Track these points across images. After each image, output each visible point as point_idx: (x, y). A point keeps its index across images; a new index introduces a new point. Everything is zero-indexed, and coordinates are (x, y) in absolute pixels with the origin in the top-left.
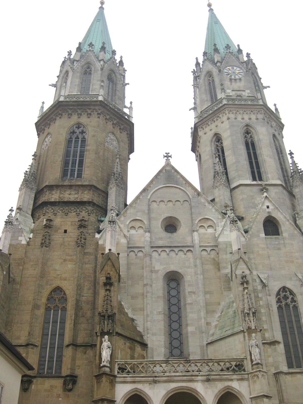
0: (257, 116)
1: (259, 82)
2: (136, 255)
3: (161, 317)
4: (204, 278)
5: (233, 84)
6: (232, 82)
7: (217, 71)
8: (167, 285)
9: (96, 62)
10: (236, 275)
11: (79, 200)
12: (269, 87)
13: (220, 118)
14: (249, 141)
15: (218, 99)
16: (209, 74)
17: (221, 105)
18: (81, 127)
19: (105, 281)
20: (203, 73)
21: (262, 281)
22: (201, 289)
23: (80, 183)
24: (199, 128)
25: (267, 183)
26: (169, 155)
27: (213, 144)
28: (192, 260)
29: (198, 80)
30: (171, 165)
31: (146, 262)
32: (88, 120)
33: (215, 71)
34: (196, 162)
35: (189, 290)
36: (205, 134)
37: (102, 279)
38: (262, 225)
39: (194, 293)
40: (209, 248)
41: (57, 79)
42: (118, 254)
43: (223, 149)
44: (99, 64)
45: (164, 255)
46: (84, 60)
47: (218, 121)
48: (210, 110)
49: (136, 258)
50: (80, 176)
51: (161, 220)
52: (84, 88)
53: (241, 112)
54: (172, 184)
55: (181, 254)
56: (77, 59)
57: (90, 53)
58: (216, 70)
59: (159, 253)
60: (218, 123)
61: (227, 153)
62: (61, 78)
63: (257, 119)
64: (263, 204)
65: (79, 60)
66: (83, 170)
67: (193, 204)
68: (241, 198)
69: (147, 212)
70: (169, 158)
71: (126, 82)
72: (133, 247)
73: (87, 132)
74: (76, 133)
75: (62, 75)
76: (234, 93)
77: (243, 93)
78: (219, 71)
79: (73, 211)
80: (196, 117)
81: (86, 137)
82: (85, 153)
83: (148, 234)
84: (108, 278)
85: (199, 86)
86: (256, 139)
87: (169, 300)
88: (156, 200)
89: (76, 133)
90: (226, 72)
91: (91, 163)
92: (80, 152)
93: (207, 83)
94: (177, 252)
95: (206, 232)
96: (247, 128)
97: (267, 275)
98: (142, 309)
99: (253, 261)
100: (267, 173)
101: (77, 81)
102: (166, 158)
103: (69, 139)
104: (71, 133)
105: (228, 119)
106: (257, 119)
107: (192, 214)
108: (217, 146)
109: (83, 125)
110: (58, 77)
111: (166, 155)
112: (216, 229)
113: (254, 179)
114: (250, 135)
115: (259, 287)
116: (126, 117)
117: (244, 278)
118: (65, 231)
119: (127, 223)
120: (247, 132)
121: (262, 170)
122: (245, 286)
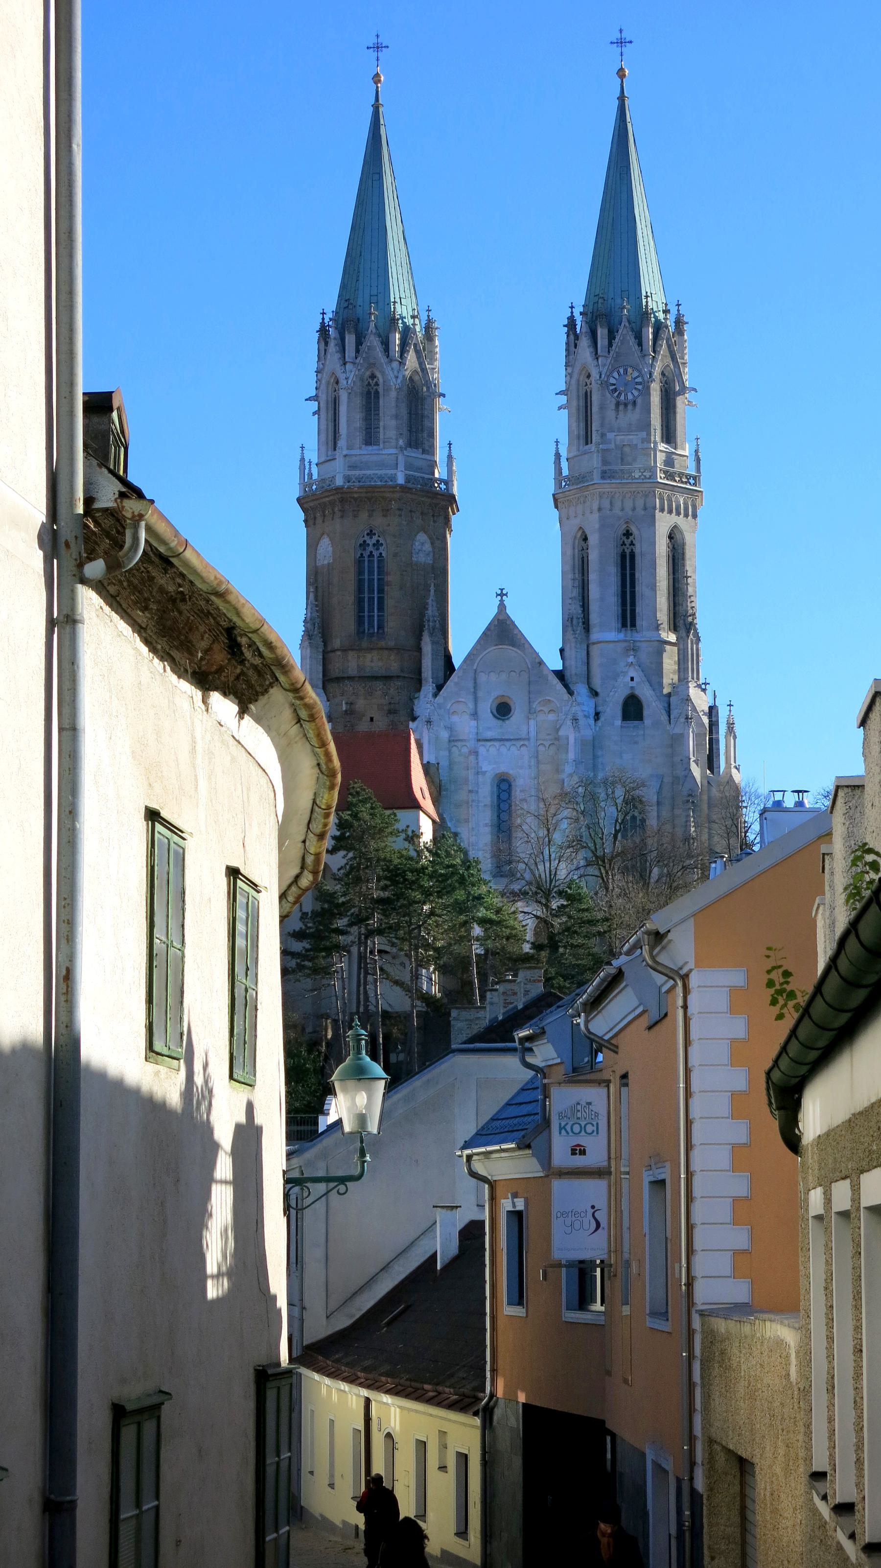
2: (460, 751)
3: (488, 830)
5: (621, 414)
14: (628, 551)
26: (504, 592)
27: (577, 541)
42: (438, 764)
45: (493, 750)
55: (513, 749)
64: (625, 673)
69: (472, 690)
72: (456, 741)
86: (637, 550)
87: (499, 806)
93: (582, 393)
98: (467, 821)
99: (600, 760)
102: (499, 598)
105: (600, 509)
111: (499, 592)
113: (624, 625)
118: (372, 719)
120: (628, 534)
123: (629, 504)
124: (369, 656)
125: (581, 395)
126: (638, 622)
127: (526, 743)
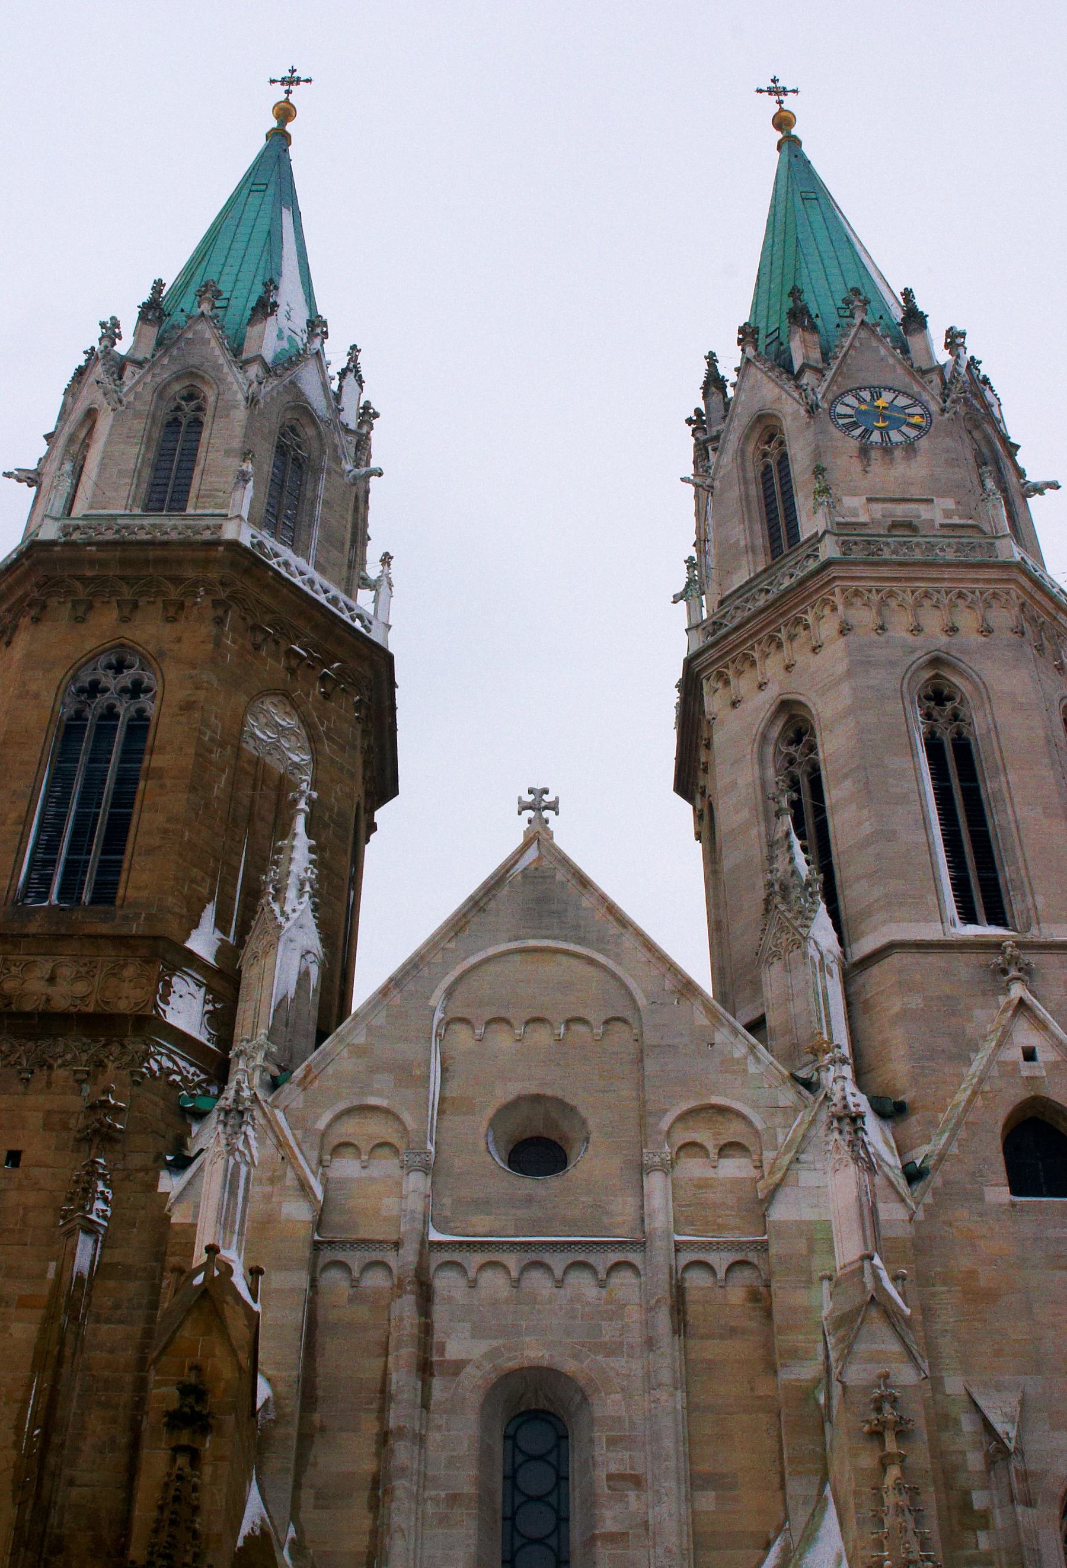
0: (984, 619)
1: (1006, 461)
2: (355, 1283)
4: (691, 1407)
6: (869, 460)
7: (803, 412)
8: (506, 1437)
9: (226, 369)
10: (845, 1387)
11: (91, 1009)
12: (1055, 486)
13: (807, 627)
14: (947, 738)
15: (802, 540)
16: (767, 428)
17: (812, 565)
18: (131, 667)
19: (175, 1405)
20: (736, 423)
21: (987, 1426)
22: (672, 1464)
23: (104, 929)
24: (708, 679)
25: (1029, 937)
27: (770, 750)
28: (634, 1315)
29: (710, 452)
30: (553, 846)
31: (401, 1319)
32: (167, 631)
33: (791, 412)
34: (698, 846)
35: (613, 1468)
36: (734, 704)
37: (164, 1394)
38: (998, 1143)
39: (637, 1481)
40: (724, 1254)
41: (43, 448)
43: (819, 778)
44: (240, 376)
45: (494, 1283)
46: (173, 360)
47: (795, 644)
48: (761, 590)
49: (351, 1300)
50: (105, 893)
51: (490, 1112)
52: (162, 488)
53: (910, 599)
54: (555, 938)
56: (140, 356)
57: (201, 326)
58: (796, 405)
59: (471, 1274)
60: (798, 652)
61: (834, 792)
62: (62, 441)
63: (987, 631)
65: (146, 360)
66: (126, 865)
67: (650, 1038)
68: (896, 1009)
70: (546, 814)
71: (374, 464)
72: (343, 1244)
73: (158, 688)
74: (106, 690)
75: (67, 430)
76: (878, 509)
77: (924, 512)
78: (808, 412)
79: (60, 1061)
80: (697, 627)
81: (151, 710)
82: (141, 785)
83: (417, 1182)
84: (194, 1392)
85: (717, 484)
87: (510, 1518)
88: (467, 1017)
89: (106, 690)
90: (846, 416)
91: (166, 831)
92: (120, 781)
93: (753, 472)
94: (558, 1273)
95: (710, 1173)
96: (937, 676)
97: (1019, 1395)
100: (1028, 891)
101: (132, 455)
102: (530, 814)
103: (70, 719)
104: (81, 691)
105: (845, 630)
106: (987, 631)
107: (641, 1086)
108: (792, 762)
109: (137, 652)
110: (48, 437)
111: (530, 798)
112: (761, 1161)
114: (949, 705)
115: (975, 1461)
116: (357, 624)
117: (887, 1407)
118: (14, 1158)
119: (322, 1124)
121: (1007, 873)
122: (891, 1445)
123: (933, 621)
124: (44, 967)
125: (751, 475)
126: (1016, 905)
127: (635, 1258)
